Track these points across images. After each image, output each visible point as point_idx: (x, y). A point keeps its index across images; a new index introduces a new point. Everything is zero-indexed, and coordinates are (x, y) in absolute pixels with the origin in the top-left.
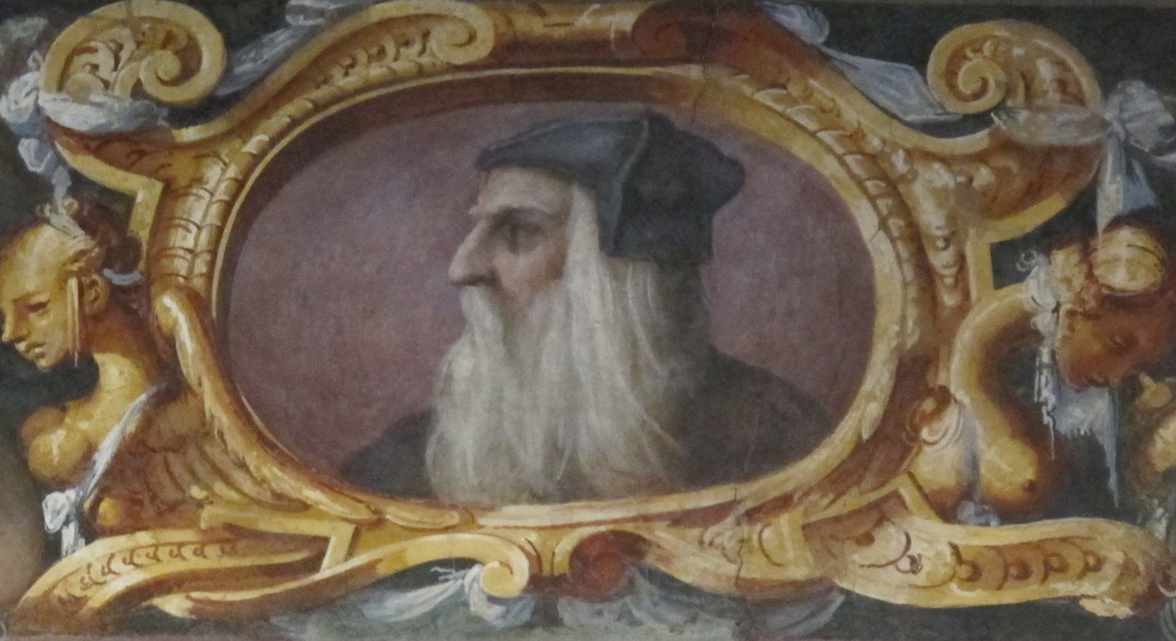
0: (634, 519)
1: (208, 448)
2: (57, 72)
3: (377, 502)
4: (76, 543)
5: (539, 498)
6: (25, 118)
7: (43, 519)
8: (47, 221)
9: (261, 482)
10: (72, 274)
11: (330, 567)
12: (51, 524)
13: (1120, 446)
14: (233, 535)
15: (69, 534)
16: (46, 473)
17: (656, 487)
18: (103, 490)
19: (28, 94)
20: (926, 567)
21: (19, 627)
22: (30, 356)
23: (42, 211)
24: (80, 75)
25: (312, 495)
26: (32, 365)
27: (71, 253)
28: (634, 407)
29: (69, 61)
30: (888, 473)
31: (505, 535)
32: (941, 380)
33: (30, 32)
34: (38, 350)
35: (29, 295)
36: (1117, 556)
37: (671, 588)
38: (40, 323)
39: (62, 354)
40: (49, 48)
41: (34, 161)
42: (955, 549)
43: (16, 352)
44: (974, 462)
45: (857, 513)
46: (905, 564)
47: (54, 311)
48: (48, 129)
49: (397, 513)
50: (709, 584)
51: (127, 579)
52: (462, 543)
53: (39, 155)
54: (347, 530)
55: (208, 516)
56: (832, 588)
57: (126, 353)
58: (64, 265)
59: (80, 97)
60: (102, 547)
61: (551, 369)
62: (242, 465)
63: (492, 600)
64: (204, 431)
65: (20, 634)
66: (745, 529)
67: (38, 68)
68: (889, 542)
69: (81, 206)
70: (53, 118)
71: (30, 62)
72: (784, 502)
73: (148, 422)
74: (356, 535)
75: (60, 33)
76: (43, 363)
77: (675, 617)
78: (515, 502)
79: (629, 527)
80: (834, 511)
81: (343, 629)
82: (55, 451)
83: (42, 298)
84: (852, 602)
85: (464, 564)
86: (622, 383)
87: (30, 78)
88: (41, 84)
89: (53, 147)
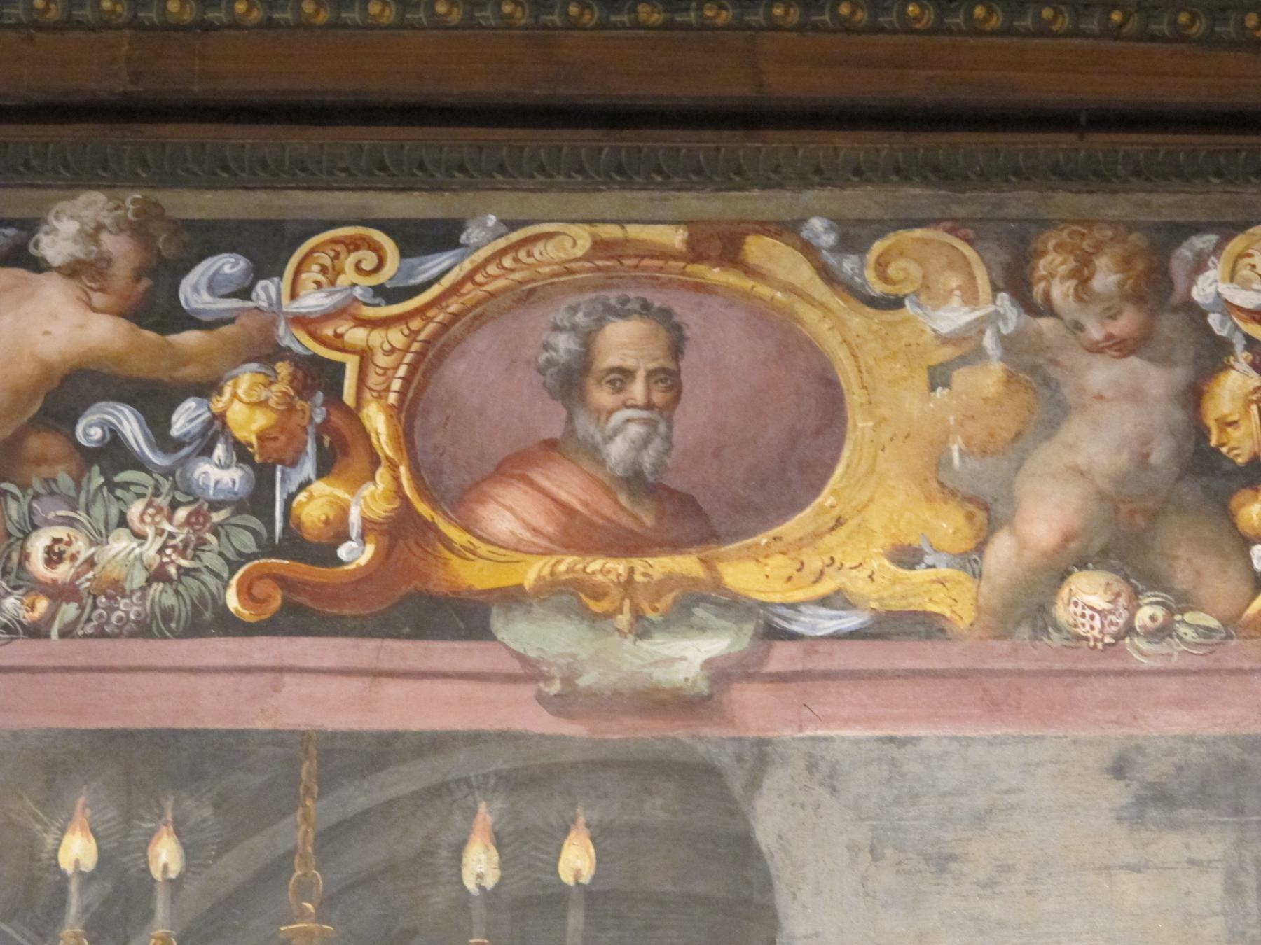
2: (1229, 269)
6: (1210, 300)
7: (1252, 563)
8: (1233, 367)
10: (1252, 402)
16: (1249, 532)
19: (1210, 285)
21: (1244, 634)
22: (1231, 456)
23: (1228, 361)
24: (1244, 272)
26: (1232, 461)
27: (1251, 388)
29: (1235, 263)
33: (1208, 244)
34: (1236, 452)
35: (1225, 416)
38: (1235, 434)
39: (1252, 454)
40: (1221, 254)
41: (1219, 328)
43: (1221, 453)
47: (1243, 428)
48: (1228, 308)
53: (1223, 325)
58: (1247, 395)
59: (1246, 285)
65: (1245, 638)
67: (1215, 268)
69: (1254, 358)
70: (1229, 300)
71: (1210, 264)
75: (1227, 244)
76: (1240, 460)
82: (1255, 518)
83: (1235, 418)
87: (1211, 274)
88: (1218, 278)
89: (1231, 319)
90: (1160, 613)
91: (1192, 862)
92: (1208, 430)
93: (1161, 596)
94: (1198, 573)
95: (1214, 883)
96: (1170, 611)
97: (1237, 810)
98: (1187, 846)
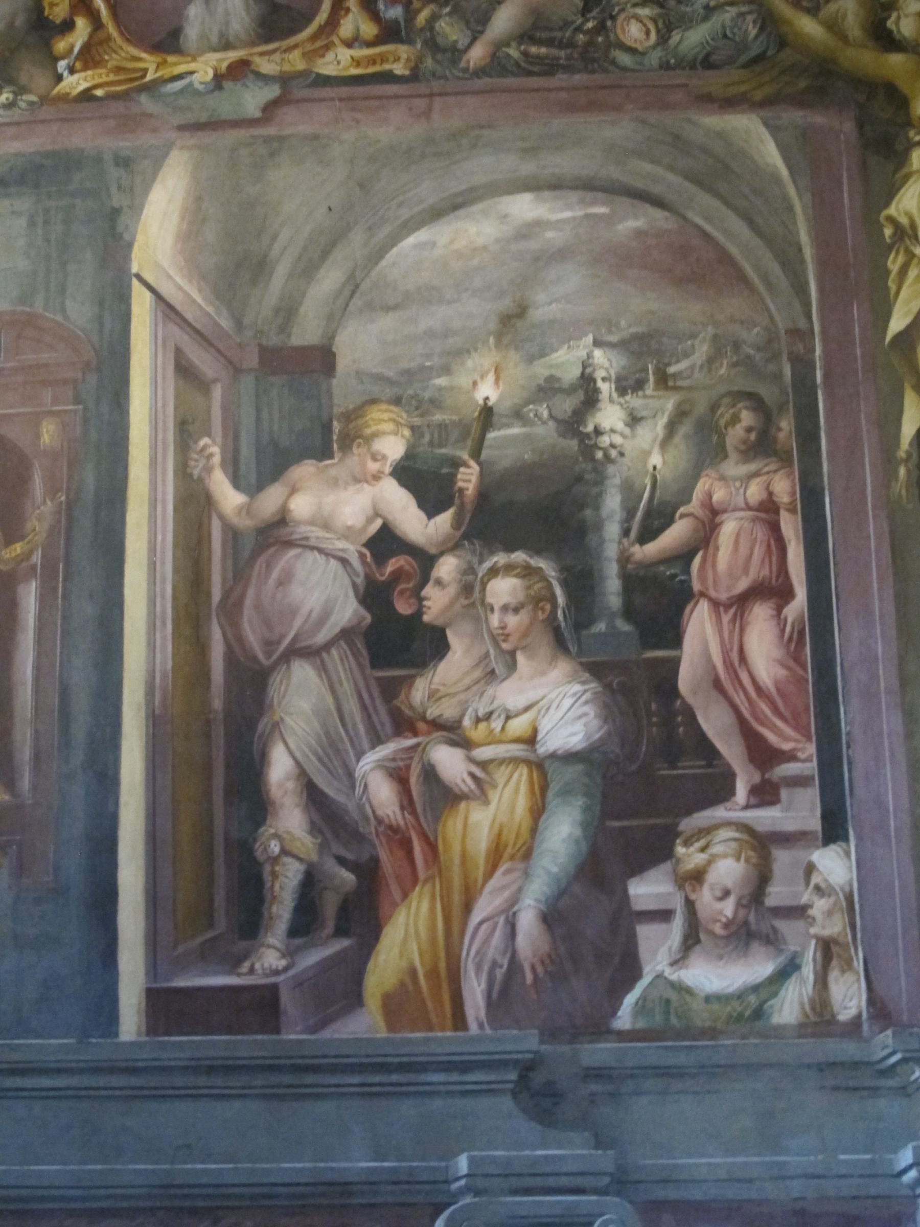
0: (247, 55)
1: (110, 44)
3: (164, 56)
4: (68, 76)
5: (215, 50)
9: (127, 53)
11: (149, 77)
12: (60, 70)
13: (406, 21)
14: (118, 69)
15: (66, 74)
17: (253, 44)
18: (77, 59)
20: (342, 63)
25: (144, 55)
26: (54, 23)
28: (247, 20)
30: (330, 34)
31: (206, 63)
32: (347, 4)
36: (404, 56)
37: (259, 76)
38: (57, 10)
42: (352, 58)
44: (358, 30)
45: (321, 47)
46: (336, 63)
47: (61, 6)
49: (171, 59)
50: (272, 73)
51: (84, 85)
52: (192, 66)
54: (154, 66)
55: (110, 65)
56: (311, 72)
57: (84, 16)
60: (76, 77)
61: (220, 10)
62: (121, 48)
63: (201, 83)
64: (109, 38)
66: (283, 56)
68: (330, 56)
72: (296, 46)
73: (91, 36)
74: (158, 67)
77: (260, 84)
78: (209, 52)
79: (245, 58)
80: (312, 48)
81: (153, 96)
84: (318, 75)
85: (192, 73)
86: (243, 13)
90: (11, 96)
91: (13, 212)
92: (44, 8)
93: (12, 88)
94: (32, 76)
95: (22, 222)
96: (16, 94)
97: (37, 186)
98: (12, 205)
